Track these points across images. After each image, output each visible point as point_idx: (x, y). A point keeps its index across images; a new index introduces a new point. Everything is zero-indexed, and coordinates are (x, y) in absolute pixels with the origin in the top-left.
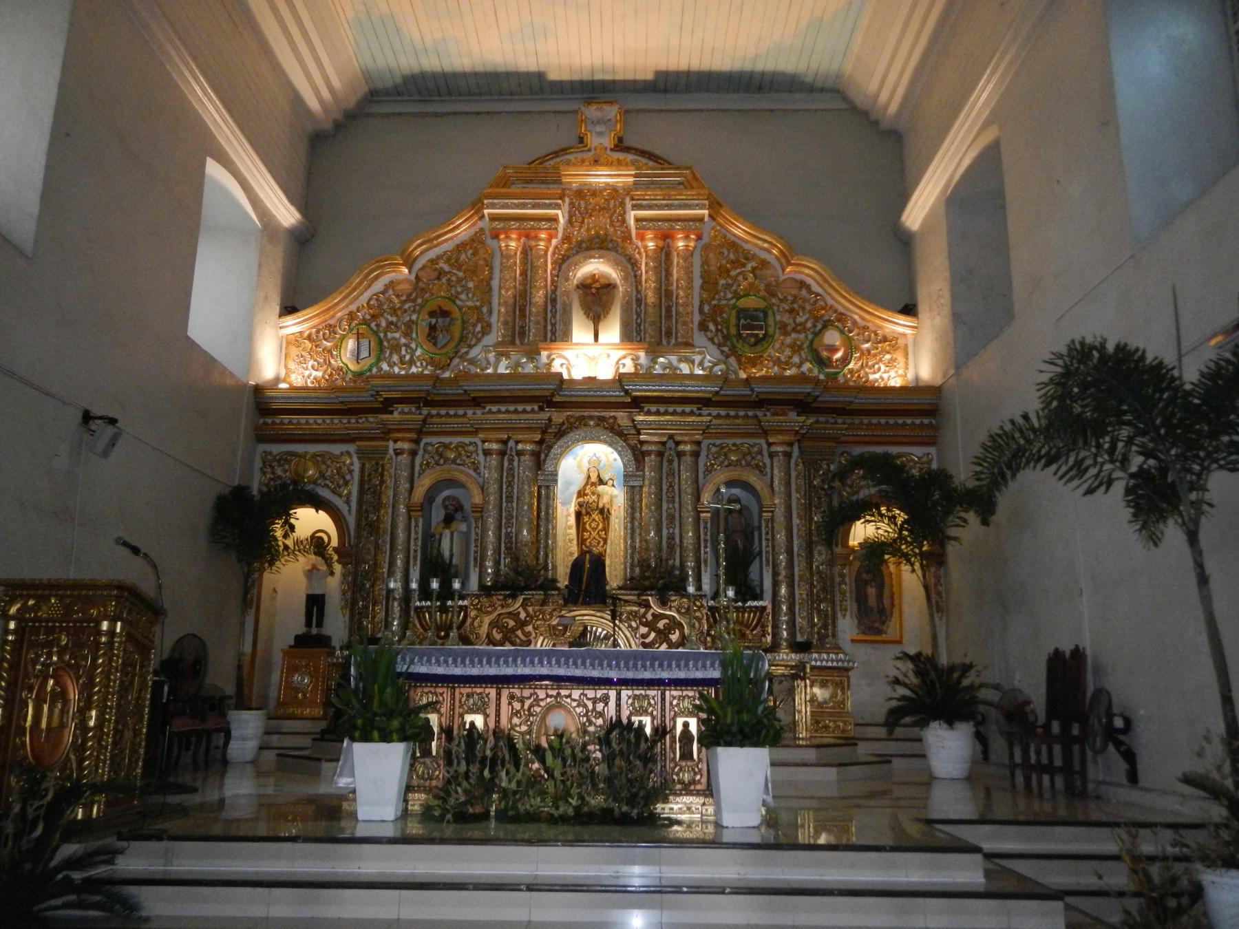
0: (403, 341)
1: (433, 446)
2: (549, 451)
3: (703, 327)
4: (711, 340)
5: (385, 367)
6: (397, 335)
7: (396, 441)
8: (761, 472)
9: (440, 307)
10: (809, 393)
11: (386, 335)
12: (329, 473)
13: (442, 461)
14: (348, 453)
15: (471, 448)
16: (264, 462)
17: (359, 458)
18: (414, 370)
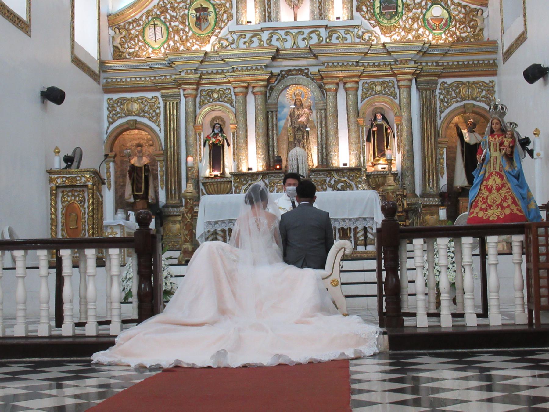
0: (181, 27)
1: (206, 91)
2: (272, 91)
3: (359, 9)
4: (363, 17)
5: (171, 43)
6: (177, 23)
7: (184, 90)
8: (394, 97)
9: (201, 5)
10: (420, 51)
11: (170, 24)
12: (146, 109)
13: (211, 100)
14: (155, 96)
15: (227, 92)
16: (109, 104)
17: (162, 99)
18: (189, 44)
